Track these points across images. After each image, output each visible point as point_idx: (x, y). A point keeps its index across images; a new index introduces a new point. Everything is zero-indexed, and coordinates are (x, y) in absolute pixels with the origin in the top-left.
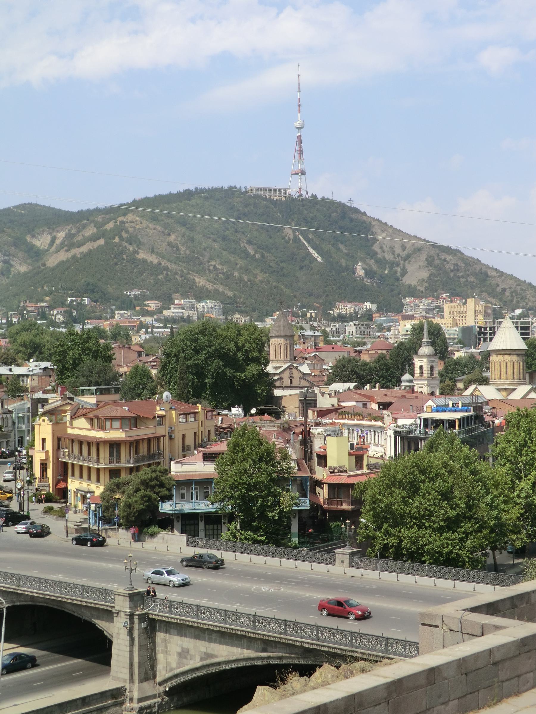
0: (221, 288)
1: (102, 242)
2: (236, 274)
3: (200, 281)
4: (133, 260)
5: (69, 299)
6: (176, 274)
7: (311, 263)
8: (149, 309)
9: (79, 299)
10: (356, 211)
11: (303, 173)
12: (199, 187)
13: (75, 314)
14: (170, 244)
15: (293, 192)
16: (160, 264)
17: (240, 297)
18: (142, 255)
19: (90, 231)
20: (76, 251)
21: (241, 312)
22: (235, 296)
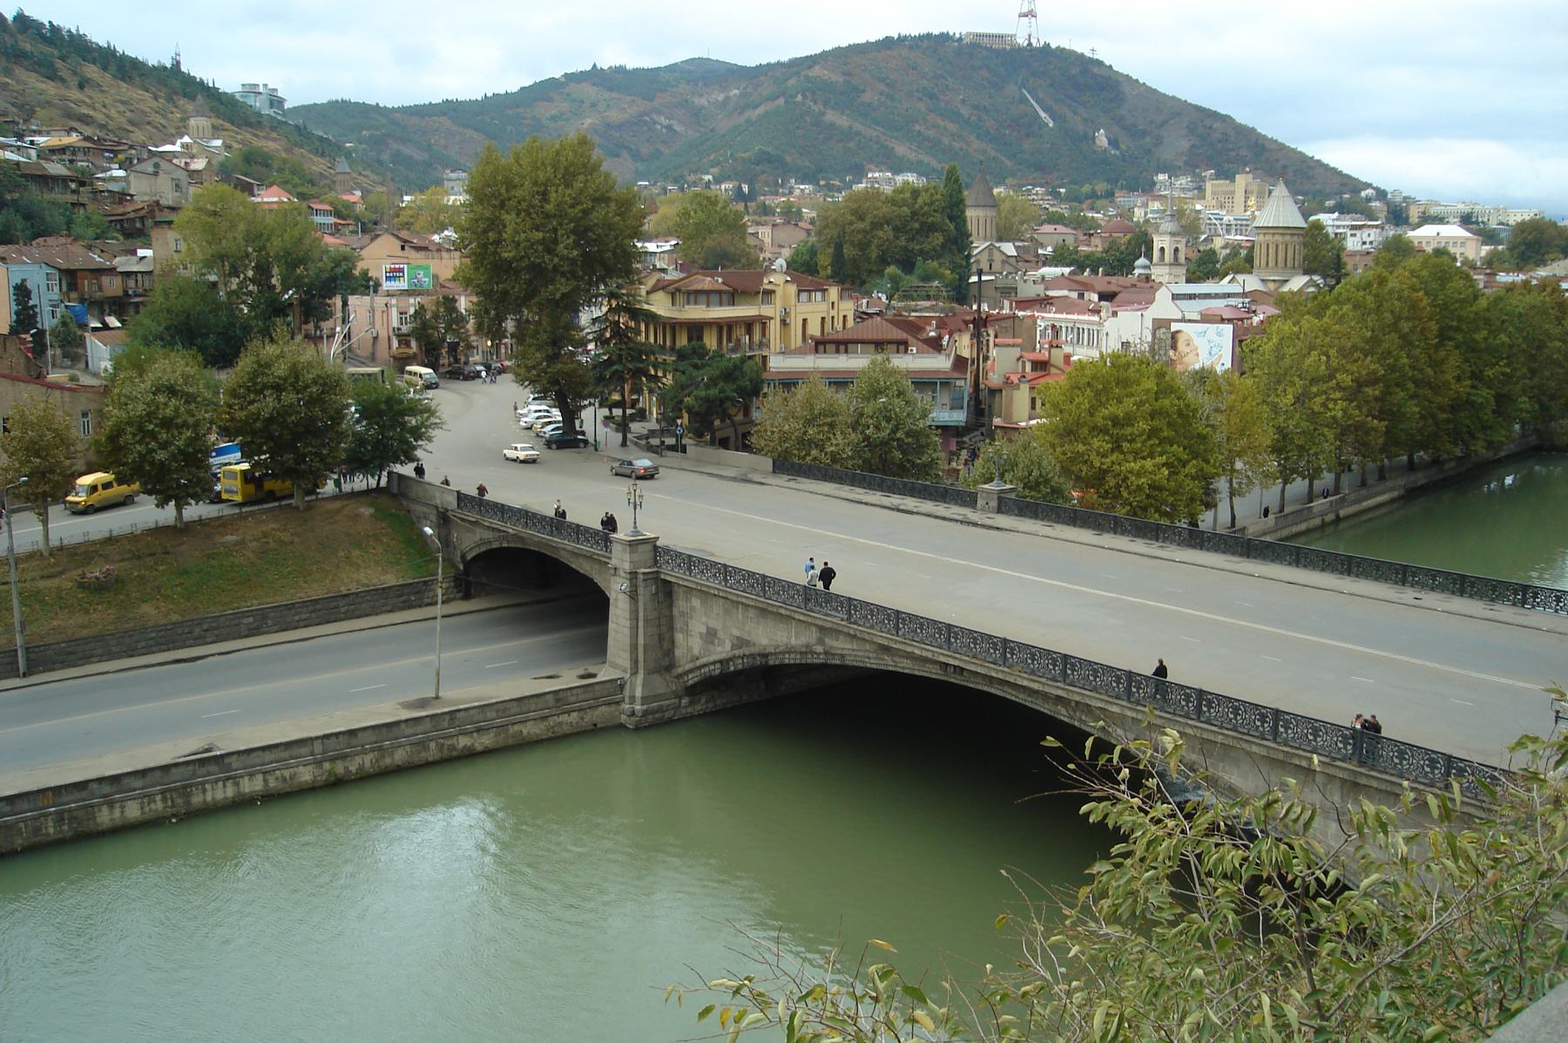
0: (926, 159)
1: (781, 101)
3: (901, 150)
7: (1040, 128)
10: (1099, 63)
12: (903, 34)
15: (1021, 41)
16: (850, 128)
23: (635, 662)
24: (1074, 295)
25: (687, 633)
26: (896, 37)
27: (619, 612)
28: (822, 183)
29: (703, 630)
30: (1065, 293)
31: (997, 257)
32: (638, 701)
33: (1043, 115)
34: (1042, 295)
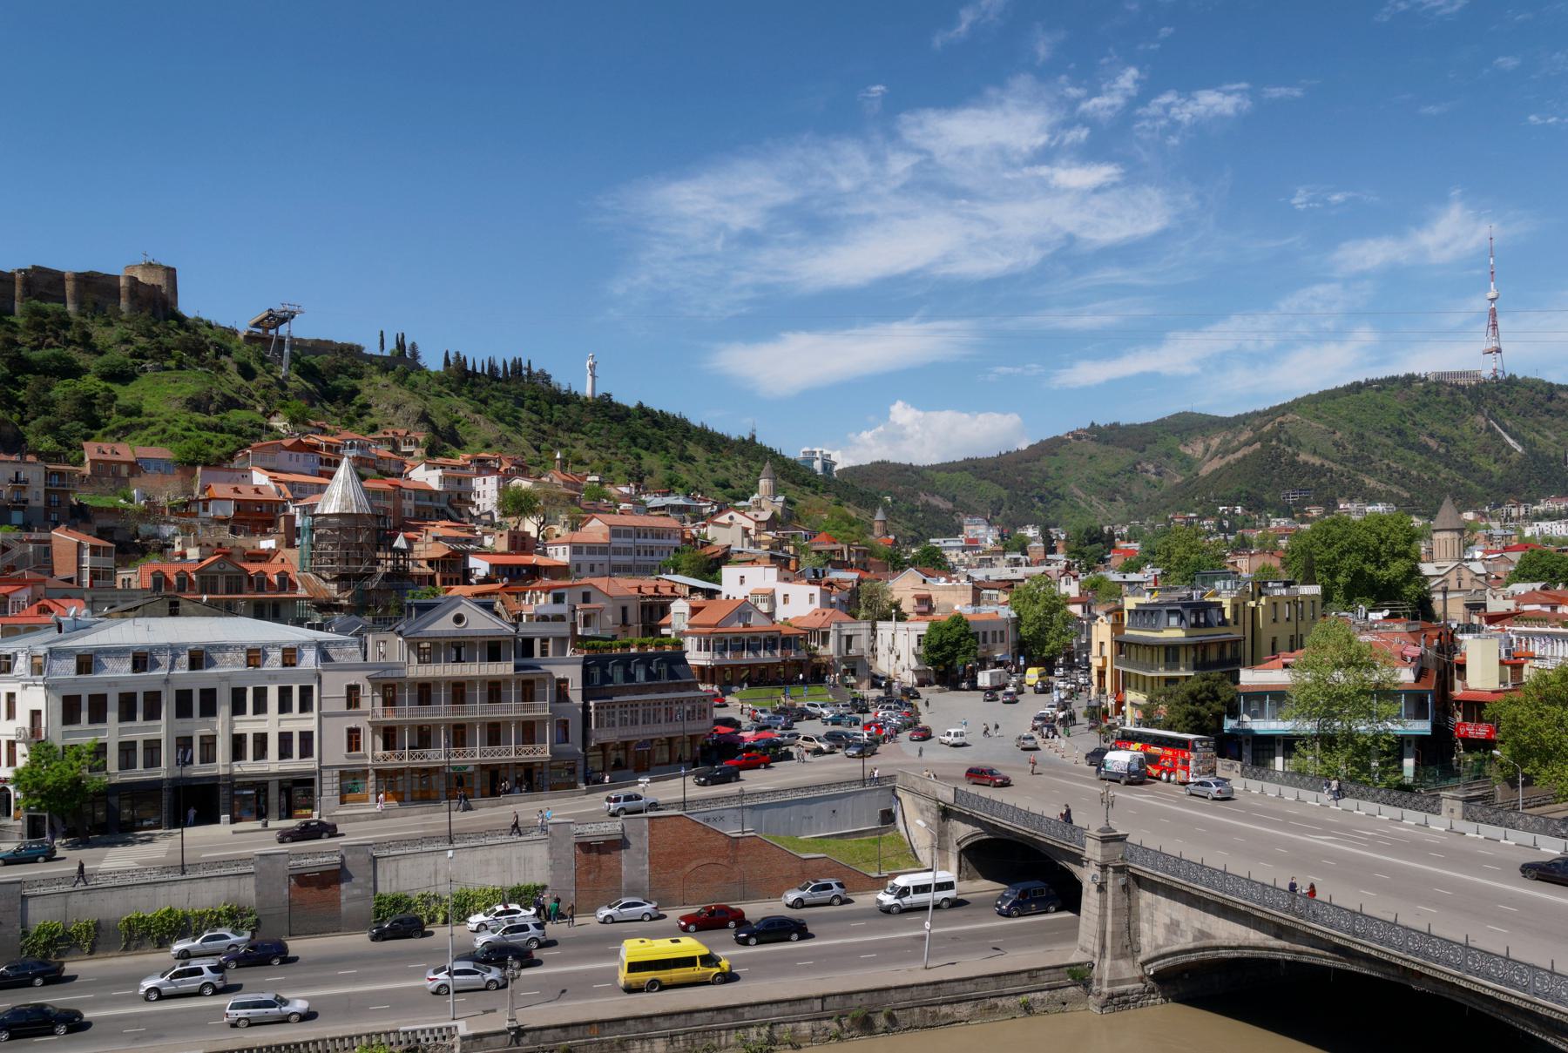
1: (1258, 445)
2: (1414, 473)
3: (1371, 482)
4: (1293, 463)
5: (1221, 508)
6: (1342, 475)
8: (1310, 516)
9: (1231, 509)
11: (1499, 351)
12: (1370, 378)
13: (1226, 524)
14: (1335, 444)
15: (1486, 373)
16: (1323, 465)
17: (1418, 498)
18: (1303, 457)
19: (1246, 435)
20: (1231, 458)
21: (1419, 515)
22: (1411, 496)
23: (1103, 947)
24: (1548, 609)
25: (1152, 922)
26: (1363, 381)
27: (1090, 901)
28: (1296, 515)
29: (1167, 921)
30: (1538, 607)
31: (1466, 576)
32: (1105, 983)
33: (1511, 441)
34: (1513, 610)
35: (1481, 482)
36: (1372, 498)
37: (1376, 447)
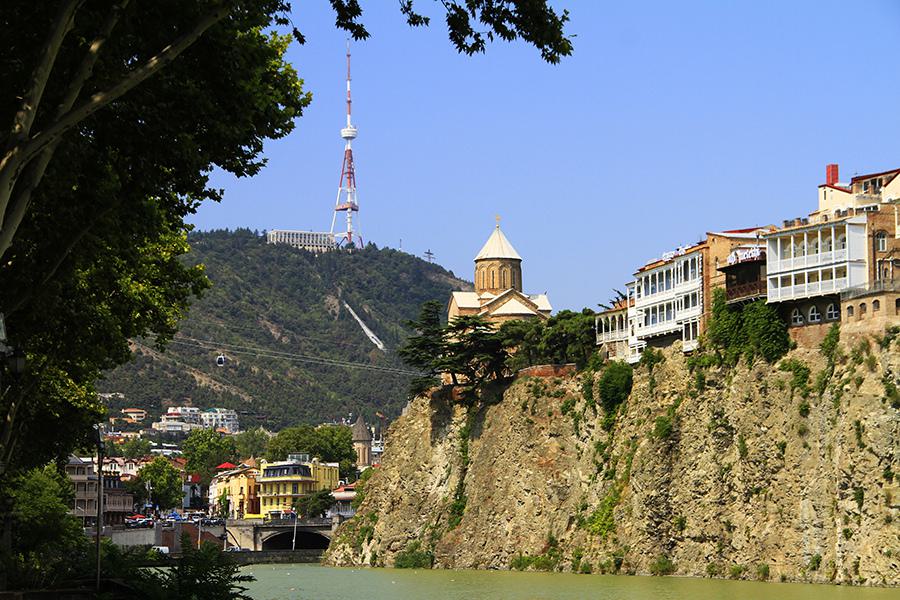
2: (255, 369)
3: (202, 380)
6: (165, 368)
7: (367, 351)
8: (129, 421)
10: (438, 269)
15: (338, 237)
17: (263, 404)
22: (254, 400)
35: (335, 387)
36: (206, 401)
37: (206, 331)
